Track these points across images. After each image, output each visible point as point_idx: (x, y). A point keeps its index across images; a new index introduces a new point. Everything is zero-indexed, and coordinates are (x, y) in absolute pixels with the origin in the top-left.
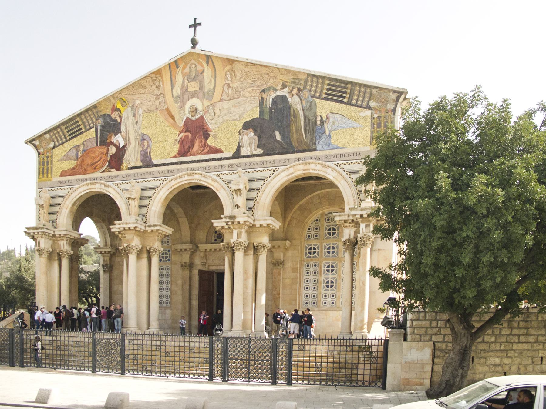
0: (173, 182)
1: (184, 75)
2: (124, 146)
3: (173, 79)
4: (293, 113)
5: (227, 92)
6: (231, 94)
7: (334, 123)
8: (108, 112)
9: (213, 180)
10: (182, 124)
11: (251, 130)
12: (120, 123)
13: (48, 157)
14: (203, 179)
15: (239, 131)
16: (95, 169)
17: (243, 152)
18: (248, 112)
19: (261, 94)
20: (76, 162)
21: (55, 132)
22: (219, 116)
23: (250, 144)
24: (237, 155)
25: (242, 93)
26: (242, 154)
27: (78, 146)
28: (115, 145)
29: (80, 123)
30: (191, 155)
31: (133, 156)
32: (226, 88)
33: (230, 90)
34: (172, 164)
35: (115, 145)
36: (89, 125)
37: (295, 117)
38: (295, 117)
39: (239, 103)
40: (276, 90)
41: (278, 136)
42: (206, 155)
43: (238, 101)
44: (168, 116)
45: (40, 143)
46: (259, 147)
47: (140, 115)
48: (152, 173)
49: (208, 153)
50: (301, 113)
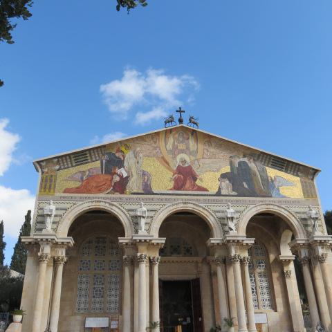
0: (171, 208)
2: (127, 177)
3: (167, 139)
7: (279, 182)
8: (114, 152)
9: (204, 209)
10: (175, 168)
12: (123, 160)
13: (52, 176)
14: (197, 208)
16: (100, 191)
17: (223, 192)
20: (80, 183)
21: (64, 158)
23: (227, 188)
24: (219, 194)
27: (84, 171)
28: (119, 176)
29: (88, 155)
30: (184, 190)
31: (135, 184)
32: (205, 151)
34: (170, 194)
35: (119, 176)
36: (96, 157)
41: (246, 186)
44: (164, 162)
45: (47, 164)
46: (233, 190)
48: (153, 199)
49: (195, 190)
50: (258, 173)
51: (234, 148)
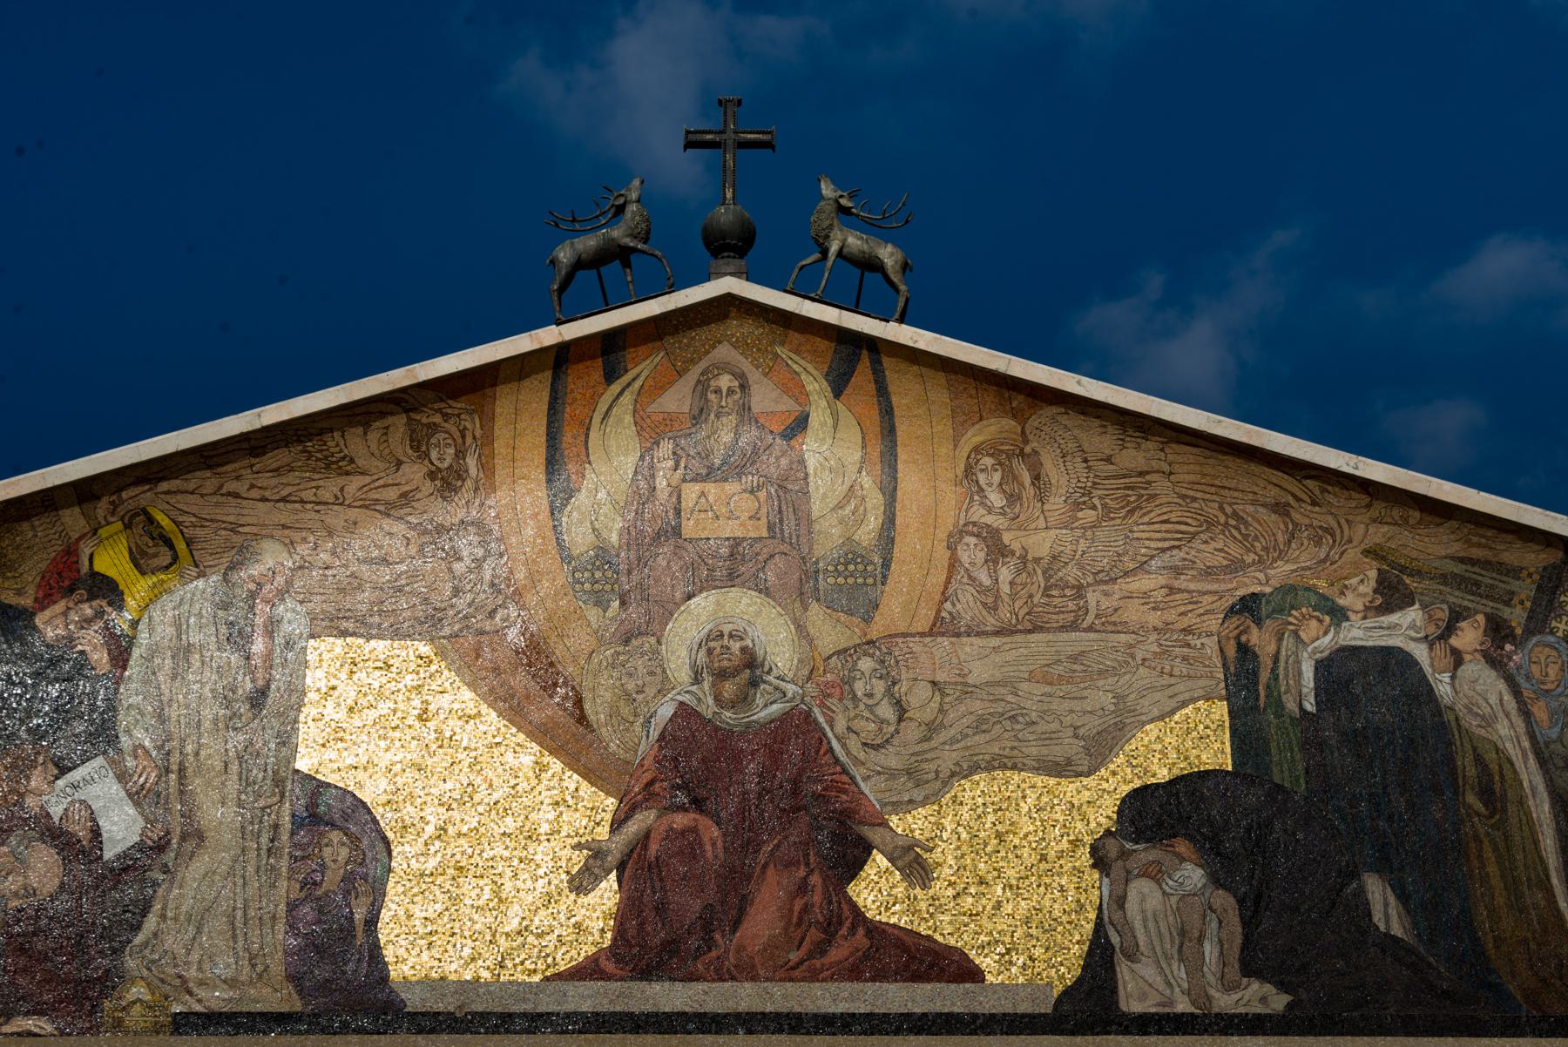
1: (651, 431)
3: (568, 437)
4: (1471, 772)
5: (987, 581)
6: (1013, 596)
10: (646, 745)
11: (1182, 846)
15: (1094, 850)
18: (1153, 729)
19: (1235, 621)
22: (932, 728)
23: (1187, 940)
25: (1092, 597)
26: (1133, 1003)
32: (972, 552)
33: (1005, 574)
37: (1487, 793)
38: (1487, 793)
39: (1074, 659)
40: (1339, 615)
42: (848, 987)
43: (1069, 650)
47: (288, 645)
50: (1530, 775)
51: (1280, 509)
